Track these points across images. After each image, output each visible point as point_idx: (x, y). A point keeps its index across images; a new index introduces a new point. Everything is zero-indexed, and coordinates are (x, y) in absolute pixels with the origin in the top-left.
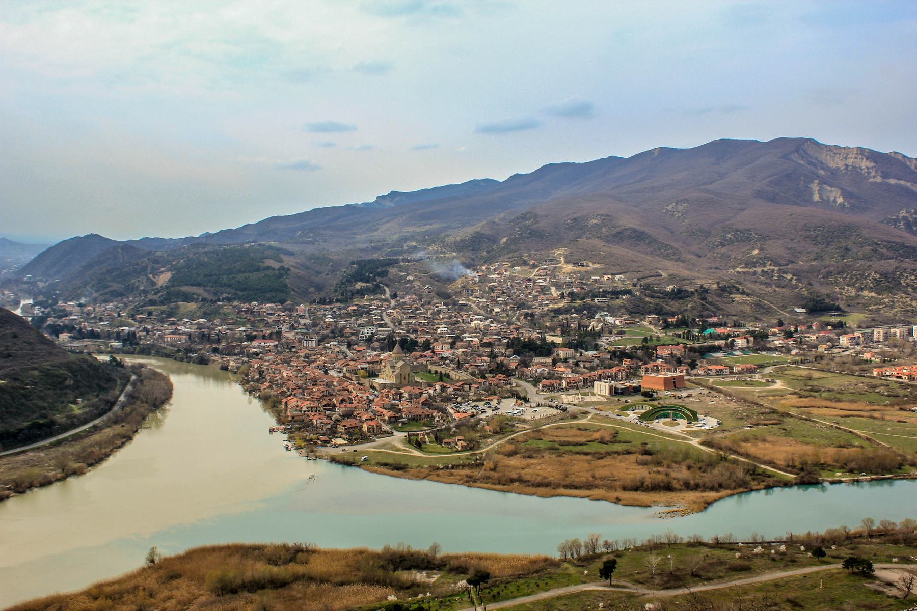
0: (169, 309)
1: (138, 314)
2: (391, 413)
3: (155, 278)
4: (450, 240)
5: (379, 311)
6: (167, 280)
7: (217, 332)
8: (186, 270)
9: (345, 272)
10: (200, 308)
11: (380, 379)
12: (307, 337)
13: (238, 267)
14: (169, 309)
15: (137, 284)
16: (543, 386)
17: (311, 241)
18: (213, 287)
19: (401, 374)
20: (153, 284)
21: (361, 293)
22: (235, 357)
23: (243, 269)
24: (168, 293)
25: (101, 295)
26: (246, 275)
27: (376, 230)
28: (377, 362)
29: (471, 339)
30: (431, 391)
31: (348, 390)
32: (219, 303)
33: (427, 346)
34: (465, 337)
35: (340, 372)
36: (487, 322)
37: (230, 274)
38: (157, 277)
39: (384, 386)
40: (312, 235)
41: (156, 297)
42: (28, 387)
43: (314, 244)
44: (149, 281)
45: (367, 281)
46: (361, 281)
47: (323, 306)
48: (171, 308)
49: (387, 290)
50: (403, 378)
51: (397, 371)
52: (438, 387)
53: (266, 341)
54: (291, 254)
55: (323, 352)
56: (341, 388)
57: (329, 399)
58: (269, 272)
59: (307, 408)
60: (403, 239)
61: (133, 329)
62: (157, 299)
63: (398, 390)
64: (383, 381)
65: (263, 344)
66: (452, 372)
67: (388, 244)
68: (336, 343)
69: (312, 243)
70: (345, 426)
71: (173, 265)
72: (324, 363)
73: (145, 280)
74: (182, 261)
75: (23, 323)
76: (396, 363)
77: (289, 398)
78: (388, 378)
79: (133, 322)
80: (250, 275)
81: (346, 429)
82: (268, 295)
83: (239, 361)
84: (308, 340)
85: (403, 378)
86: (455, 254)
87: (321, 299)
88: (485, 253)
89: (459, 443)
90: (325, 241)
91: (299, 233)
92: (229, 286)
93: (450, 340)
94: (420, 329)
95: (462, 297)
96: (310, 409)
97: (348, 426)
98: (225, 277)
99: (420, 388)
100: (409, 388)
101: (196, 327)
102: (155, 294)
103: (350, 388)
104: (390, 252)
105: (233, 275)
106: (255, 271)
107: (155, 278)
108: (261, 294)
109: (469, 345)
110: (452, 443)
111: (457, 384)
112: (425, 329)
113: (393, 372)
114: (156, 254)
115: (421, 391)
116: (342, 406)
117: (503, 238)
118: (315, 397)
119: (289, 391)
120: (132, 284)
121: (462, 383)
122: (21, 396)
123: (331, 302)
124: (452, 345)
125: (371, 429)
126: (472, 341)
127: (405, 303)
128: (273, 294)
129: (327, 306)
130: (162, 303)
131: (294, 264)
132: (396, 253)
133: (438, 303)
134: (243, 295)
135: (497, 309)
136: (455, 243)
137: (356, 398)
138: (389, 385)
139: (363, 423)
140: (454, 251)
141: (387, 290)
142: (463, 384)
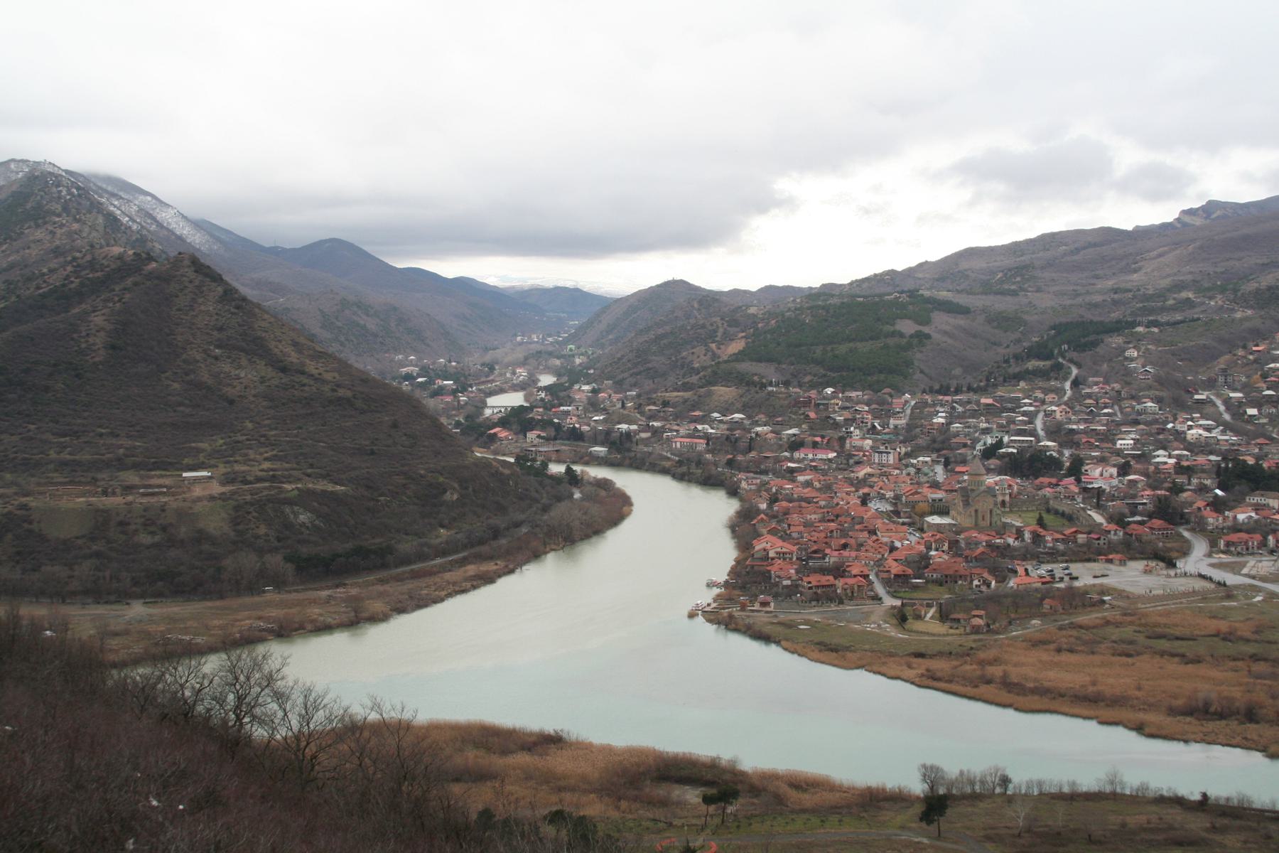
0: (696, 397)
1: (649, 405)
7: (753, 435)
10: (741, 396)
14: (696, 398)
15: (690, 358)
16: (1228, 544)
17: (1013, 291)
18: (793, 364)
24: (715, 373)
25: (631, 375)
27: (1135, 271)
32: (770, 389)
40: (1018, 279)
41: (694, 379)
42: (382, 498)
43: (1018, 295)
47: (941, 397)
50: (980, 518)
53: (816, 451)
57: (826, 543)
59: (777, 553)
61: (634, 427)
62: (695, 382)
65: (810, 456)
66: (1082, 512)
69: (1014, 293)
70: (810, 583)
72: (881, 488)
74: (773, 322)
75: (414, 407)
79: (638, 416)
80: (859, 345)
81: (810, 588)
83: (754, 481)
84: (882, 452)
85: (980, 518)
86: (1249, 312)
87: (942, 386)
90: (1039, 290)
91: (1000, 275)
96: (782, 555)
97: (814, 583)
101: (725, 426)
104: (1140, 309)
106: (872, 338)
107: (719, 349)
108: (863, 378)
110: (962, 621)
111: (1066, 532)
112: (1092, 440)
120: (682, 358)
125: (848, 591)
127: (1089, 396)
128: (882, 377)
129: (948, 398)
131: (947, 328)
138: (947, 527)
140: (1251, 307)
142: (1076, 532)
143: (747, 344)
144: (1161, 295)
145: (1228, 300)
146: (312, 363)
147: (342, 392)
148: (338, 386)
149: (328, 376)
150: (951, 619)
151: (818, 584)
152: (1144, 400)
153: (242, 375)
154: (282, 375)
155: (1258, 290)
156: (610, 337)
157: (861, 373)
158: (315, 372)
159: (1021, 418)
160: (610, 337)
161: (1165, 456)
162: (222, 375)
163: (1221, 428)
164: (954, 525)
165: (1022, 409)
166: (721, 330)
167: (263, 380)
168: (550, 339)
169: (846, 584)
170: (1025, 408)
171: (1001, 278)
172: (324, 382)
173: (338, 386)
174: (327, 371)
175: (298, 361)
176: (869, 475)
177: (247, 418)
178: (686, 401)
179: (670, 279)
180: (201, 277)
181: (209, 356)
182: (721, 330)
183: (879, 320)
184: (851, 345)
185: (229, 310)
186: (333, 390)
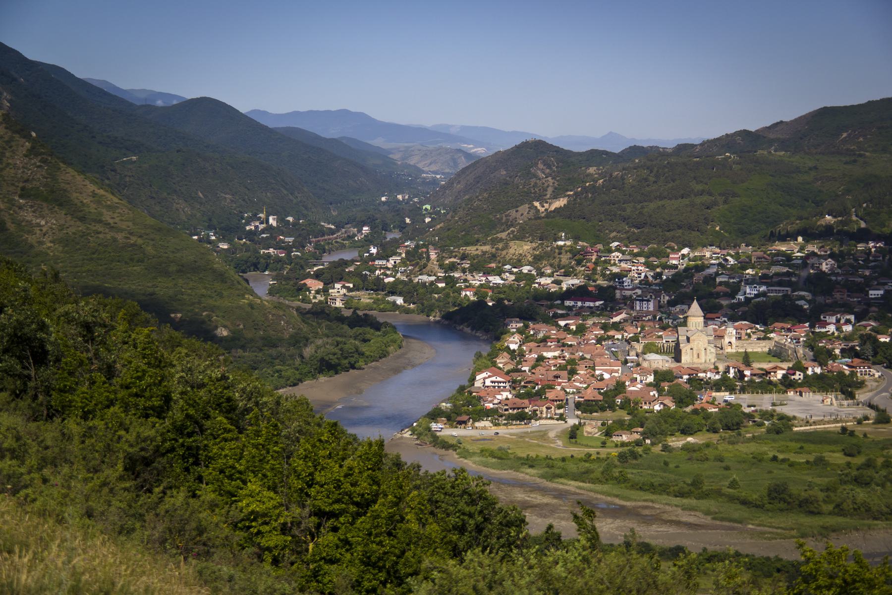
0: (494, 250)
44: (533, 211)
48: (497, 249)
59: (492, 382)
81: (506, 410)
85: (695, 356)
91: (845, 135)
114: (588, 171)
120: (506, 216)
146: (108, 213)
147: (133, 240)
148: (131, 234)
149: (123, 225)
151: (515, 406)
153: (43, 223)
154: (79, 223)
158: (111, 221)
162: (23, 224)
167: (61, 228)
171: (845, 138)
172: (120, 230)
173: (131, 234)
174: (122, 220)
175: (96, 211)
177: (42, 262)
178: (484, 253)
180: (10, 134)
181: (13, 205)
184: (660, 203)
185: (35, 164)
186: (127, 238)
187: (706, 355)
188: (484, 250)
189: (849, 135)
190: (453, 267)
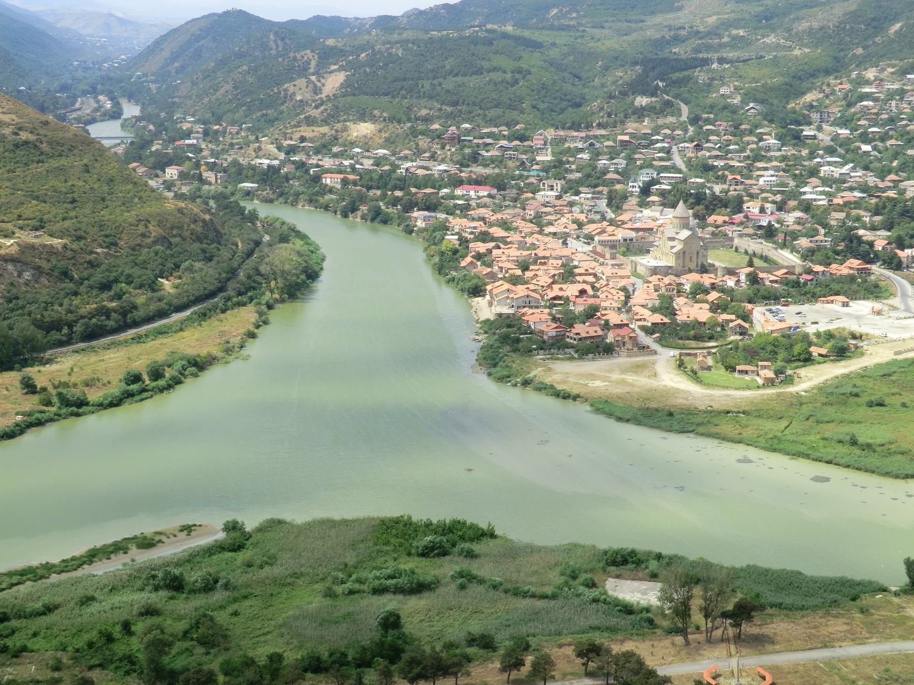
0: (333, 132)
2: (658, 318)
3: (320, 81)
4: (805, 25)
5: (666, 145)
6: (337, 85)
8: (368, 70)
9: (621, 78)
10: (380, 131)
11: (649, 260)
12: (544, 184)
13: (448, 67)
15: (292, 89)
17: (574, 26)
18: (406, 98)
19: (684, 253)
20: (317, 91)
21: (640, 113)
22: (426, 213)
23: (455, 72)
26: (459, 79)
28: (652, 229)
29: (814, 196)
30: (731, 283)
31: (595, 275)
33: (737, 206)
34: (805, 193)
35: (589, 244)
36: (846, 169)
37: (434, 78)
38: (323, 81)
39: (655, 271)
40: (574, 15)
41: (315, 113)
44: (311, 86)
45: (653, 94)
46: (644, 93)
47: (576, 134)
48: (337, 131)
49: (685, 109)
50: (688, 259)
51: (679, 247)
52: (743, 278)
54: (536, 45)
55: (566, 209)
56: (584, 272)
58: (497, 76)
60: (723, 24)
61: (276, 163)
63: (676, 279)
64: (654, 263)
66: (774, 251)
67: (698, 32)
68: (589, 196)
71: (350, 62)
72: (565, 227)
73: (305, 84)
76: (677, 233)
77: (497, 284)
78: (664, 258)
80: (465, 79)
81: (580, 339)
82: (493, 113)
85: (688, 259)
86: (807, 50)
87: (573, 123)
88: (860, 51)
89: (762, 373)
91: (555, 11)
92: (431, 97)
93: (778, 198)
94: (730, 177)
95: (809, 124)
97: (584, 335)
98: (427, 84)
99: (712, 275)
100: (695, 277)
102: (316, 107)
103: (599, 270)
105: (441, 80)
106: (474, 73)
107: (320, 81)
108: (481, 112)
109: (807, 207)
112: (738, 177)
113: (672, 247)
114: (327, 43)
115: (714, 281)
116: (579, 300)
117: (893, 25)
118: (541, 283)
119: (501, 271)
120: (285, 90)
121: (785, 271)
122: (86, 265)
123: (589, 127)
124: (781, 207)
126: (815, 200)
127: (712, 132)
129: (583, 134)
130: (325, 122)
132: (709, 48)
133: (765, 134)
134: (452, 113)
135: (866, 148)
136: (810, 32)
137: (605, 289)
139: (609, 330)
140: (807, 46)
141: (685, 109)
143: (347, 76)
144: (714, 32)
145: (783, 39)
148: (20, 129)
150: (739, 371)
152: (765, 137)
155: (811, 29)
156: (176, 64)
157: (478, 108)
159: (660, 155)
160: (176, 64)
161: (811, 193)
163: (851, 165)
164: (670, 267)
165: (656, 146)
166: (313, 63)
168: (106, 65)
169: (618, 335)
170: (659, 145)
171: (556, 13)
176: (542, 212)
178: (324, 135)
179: (230, 8)
182: (313, 63)
183: (473, 54)
187: (697, 258)
188: (323, 132)
189: (561, 11)
190: (291, 150)
